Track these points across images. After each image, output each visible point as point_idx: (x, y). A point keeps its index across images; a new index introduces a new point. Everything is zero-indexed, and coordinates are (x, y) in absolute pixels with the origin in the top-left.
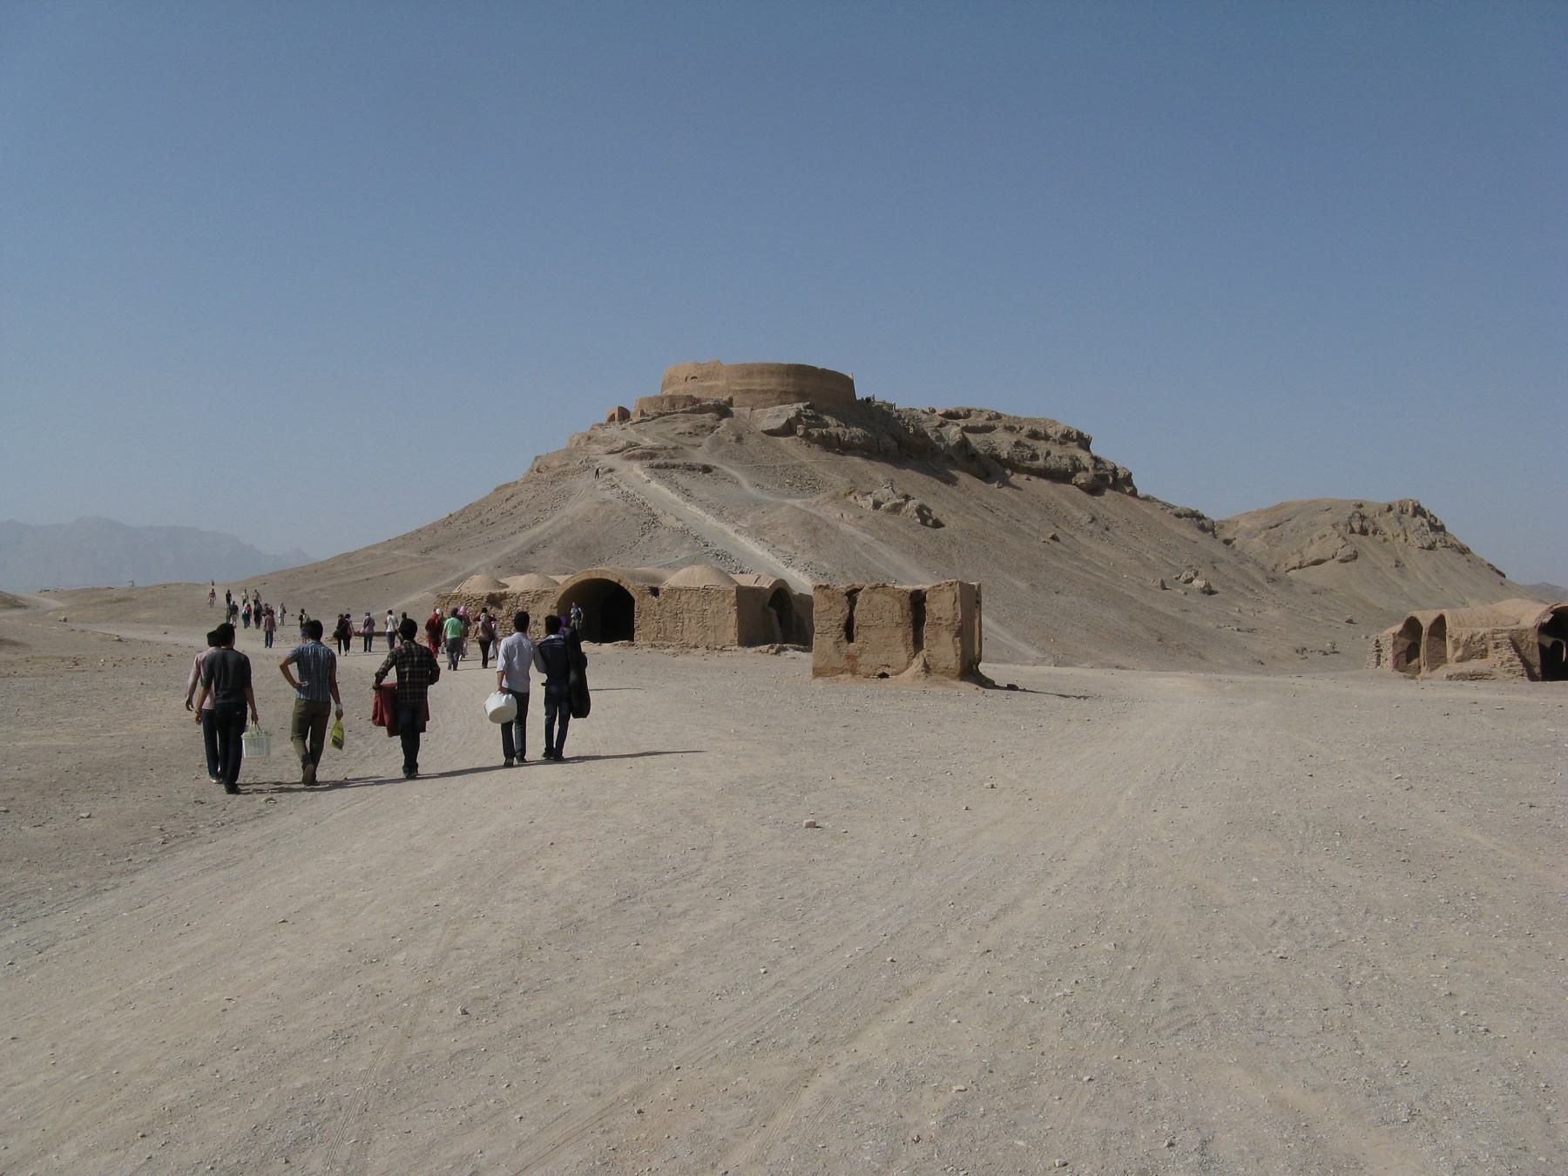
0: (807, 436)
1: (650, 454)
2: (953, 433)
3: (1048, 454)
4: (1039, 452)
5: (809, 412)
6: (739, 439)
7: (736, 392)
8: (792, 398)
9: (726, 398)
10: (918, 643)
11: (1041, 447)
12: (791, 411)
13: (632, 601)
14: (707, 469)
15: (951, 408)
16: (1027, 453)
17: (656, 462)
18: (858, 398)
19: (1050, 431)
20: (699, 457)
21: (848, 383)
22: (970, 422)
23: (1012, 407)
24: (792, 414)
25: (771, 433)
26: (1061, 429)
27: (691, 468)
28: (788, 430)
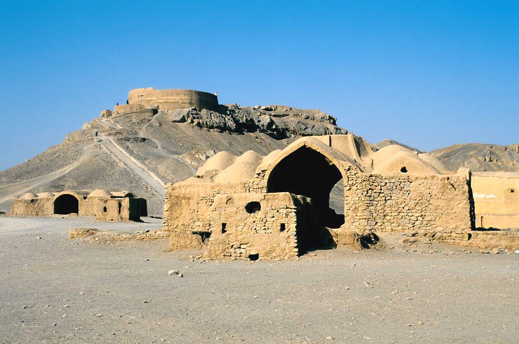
0: (192, 122)
1: (118, 133)
2: (265, 120)
3: (313, 127)
4: (309, 126)
5: (194, 112)
6: (161, 125)
7: (160, 103)
8: (187, 105)
9: (156, 105)
10: (120, 212)
11: (310, 123)
12: (185, 111)
13: (77, 201)
14: (144, 140)
15: (269, 106)
16: (304, 127)
17: (121, 136)
18: (219, 103)
19: (316, 116)
20: (142, 135)
21: (215, 98)
22: (277, 112)
23: (297, 105)
24: (186, 113)
25: (174, 122)
26: (321, 115)
27: (136, 140)
28: (183, 120)
